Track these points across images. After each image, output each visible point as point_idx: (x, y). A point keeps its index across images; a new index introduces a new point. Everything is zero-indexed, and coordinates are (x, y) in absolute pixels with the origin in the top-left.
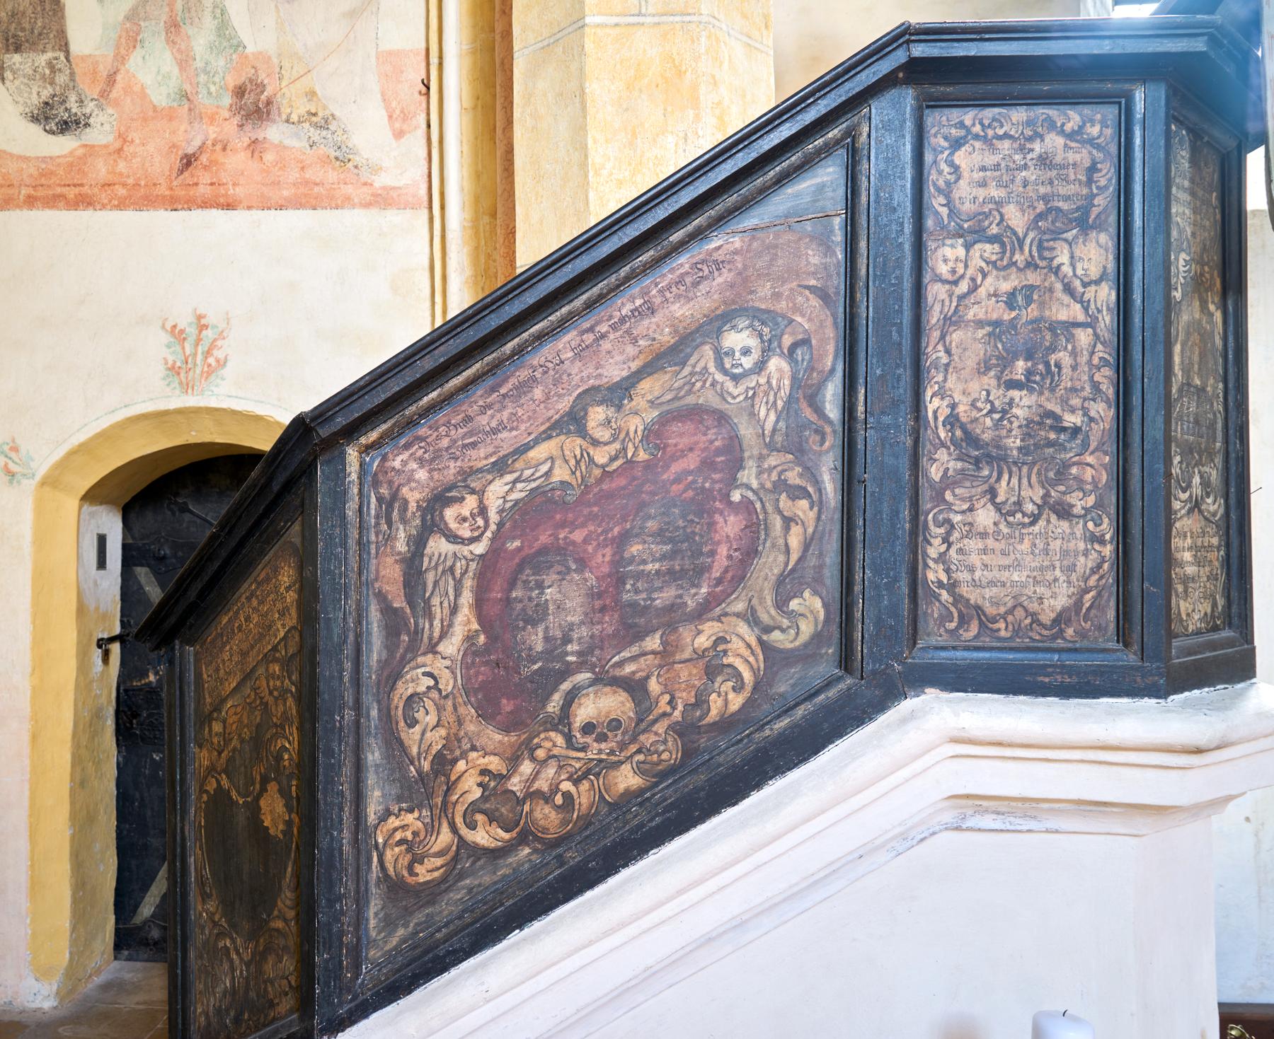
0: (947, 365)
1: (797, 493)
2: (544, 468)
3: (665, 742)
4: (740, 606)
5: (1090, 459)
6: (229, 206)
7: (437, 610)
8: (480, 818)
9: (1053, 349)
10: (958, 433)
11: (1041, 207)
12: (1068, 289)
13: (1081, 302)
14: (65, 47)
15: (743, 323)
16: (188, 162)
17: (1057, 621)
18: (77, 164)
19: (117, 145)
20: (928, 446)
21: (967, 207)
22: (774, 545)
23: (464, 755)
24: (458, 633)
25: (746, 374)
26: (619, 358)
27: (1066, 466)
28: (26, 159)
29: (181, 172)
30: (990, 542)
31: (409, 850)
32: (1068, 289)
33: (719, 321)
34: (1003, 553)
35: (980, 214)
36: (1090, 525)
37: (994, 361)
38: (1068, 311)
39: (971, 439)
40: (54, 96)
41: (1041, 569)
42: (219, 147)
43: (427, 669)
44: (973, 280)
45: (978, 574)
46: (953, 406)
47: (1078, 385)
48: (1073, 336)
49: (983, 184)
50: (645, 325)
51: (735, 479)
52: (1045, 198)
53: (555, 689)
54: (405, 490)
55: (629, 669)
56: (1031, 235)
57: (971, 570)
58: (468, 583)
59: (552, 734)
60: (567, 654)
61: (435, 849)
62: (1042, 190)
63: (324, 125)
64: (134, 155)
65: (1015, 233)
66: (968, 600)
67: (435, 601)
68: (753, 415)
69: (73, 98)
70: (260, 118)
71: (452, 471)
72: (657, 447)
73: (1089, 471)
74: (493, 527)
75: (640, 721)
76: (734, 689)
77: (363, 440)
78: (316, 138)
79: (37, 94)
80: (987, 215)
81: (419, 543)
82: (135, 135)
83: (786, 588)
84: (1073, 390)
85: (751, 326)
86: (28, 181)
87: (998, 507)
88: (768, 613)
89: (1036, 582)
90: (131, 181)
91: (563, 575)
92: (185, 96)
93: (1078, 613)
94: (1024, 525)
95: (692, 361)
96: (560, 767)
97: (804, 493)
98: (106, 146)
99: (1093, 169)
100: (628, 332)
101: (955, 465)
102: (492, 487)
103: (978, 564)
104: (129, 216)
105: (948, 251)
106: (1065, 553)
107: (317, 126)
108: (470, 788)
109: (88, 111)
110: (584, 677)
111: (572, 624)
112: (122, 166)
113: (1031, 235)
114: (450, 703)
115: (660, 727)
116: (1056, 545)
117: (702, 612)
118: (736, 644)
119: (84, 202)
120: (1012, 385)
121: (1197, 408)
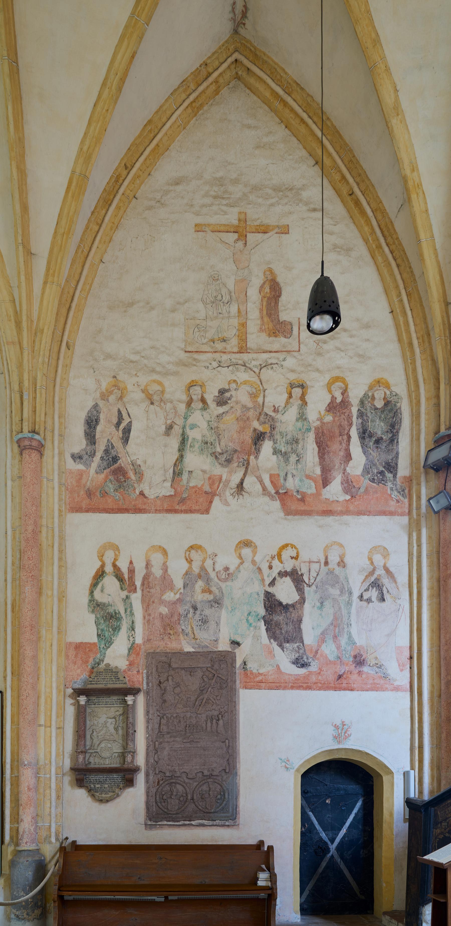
6: (352, 690)
14: (302, 642)
16: (340, 677)
18: (306, 677)
19: (319, 671)
28: (291, 675)
29: (338, 680)
42: (349, 673)
63: (380, 667)
64: (324, 674)
69: (305, 657)
70: (361, 665)
78: (378, 671)
82: (324, 669)
86: (291, 682)
90: (323, 682)
92: (339, 658)
98: (315, 672)
104: (322, 692)
107: (378, 667)
109: (310, 661)
112: (320, 678)
119: (309, 688)
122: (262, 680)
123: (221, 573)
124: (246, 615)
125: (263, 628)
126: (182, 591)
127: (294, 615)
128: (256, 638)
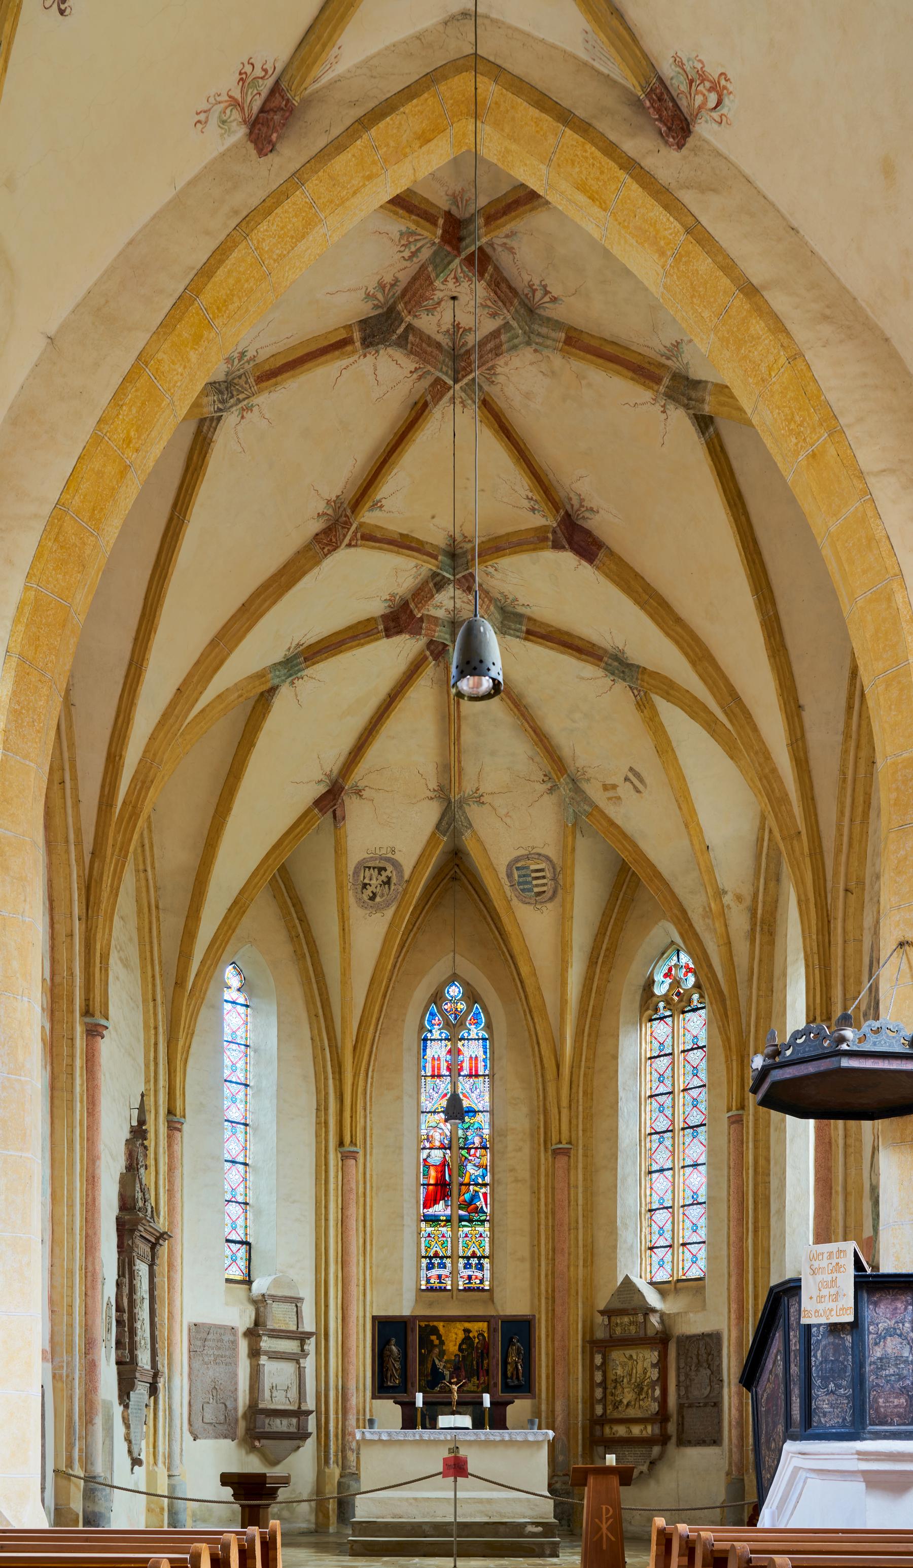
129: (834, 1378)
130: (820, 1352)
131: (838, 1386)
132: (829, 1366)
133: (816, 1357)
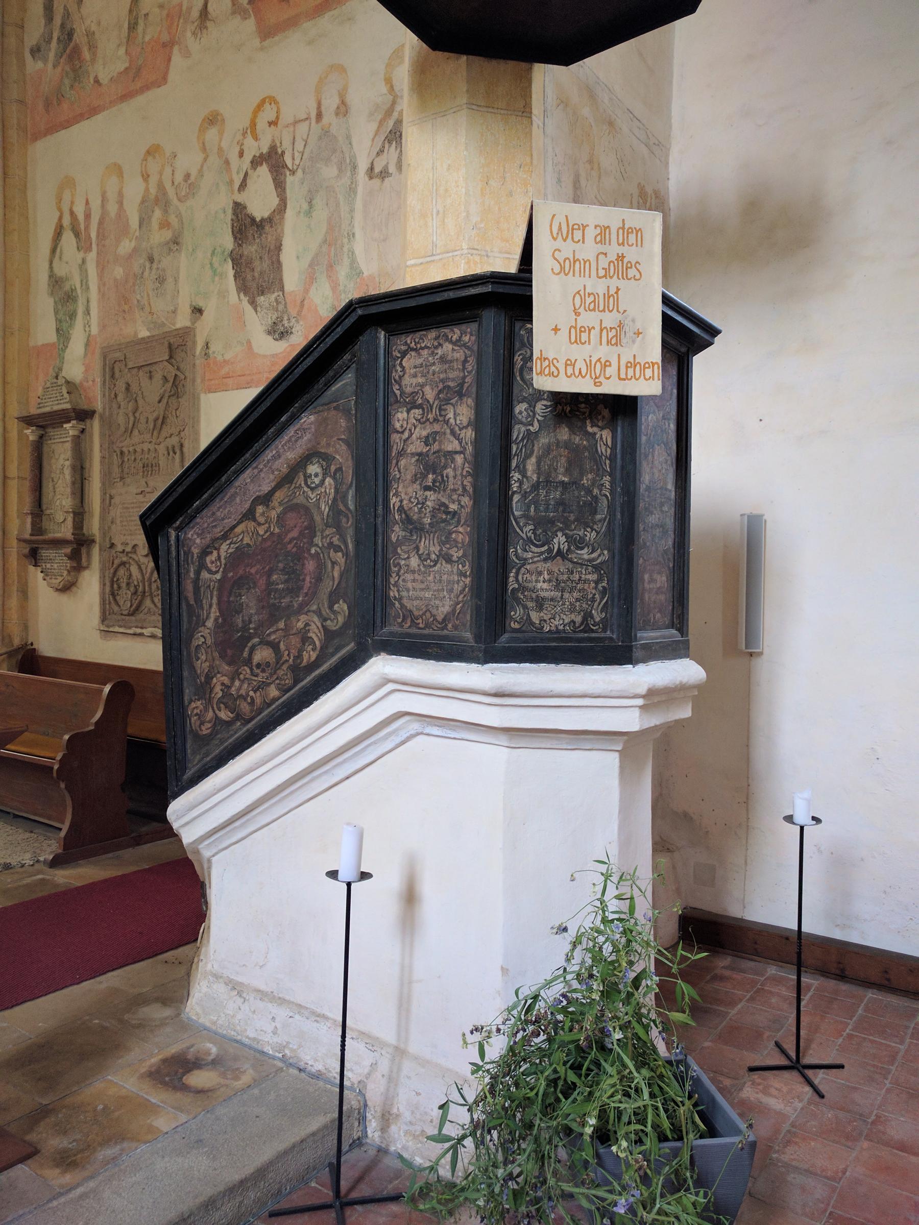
0: (399, 478)
1: (337, 549)
2: (241, 537)
3: (287, 675)
4: (314, 607)
5: (461, 529)
7: (205, 606)
8: (222, 706)
9: (445, 467)
10: (403, 516)
11: (441, 386)
12: (453, 433)
13: (458, 439)
15: (315, 460)
17: (444, 620)
20: (391, 523)
21: (408, 390)
22: (328, 576)
23: (215, 675)
24: (212, 616)
25: (317, 486)
26: (267, 481)
27: (450, 533)
30: (416, 575)
31: (199, 718)
32: (453, 433)
33: (306, 460)
34: (422, 582)
35: (413, 393)
36: (460, 566)
37: (419, 476)
38: (453, 445)
39: (408, 520)
40: (278, 318)
41: (438, 590)
43: (202, 634)
44: (410, 430)
45: (411, 593)
46: (401, 501)
47: (456, 486)
48: (454, 459)
49: (415, 376)
50: (277, 464)
51: (312, 542)
52: (442, 381)
53: (246, 646)
54: (193, 548)
55: (273, 637)
56: (436, 403)
57: (408, 590)
58: (215, 593)
59: (246, 667)
60: (250, 629)
61: (208, 719)
62: (442, 376)
65: (428, 402)
66: (406, 607)
67: (204, 602)
68: (319, 508)
69: (286, 318)
71: (209, 539)
72: (282, 526)
73: (461, 536)
74: (223, 566)
75: (278, 663)
76: (312, 649)
77: (174, 525)
79: (271, 317)
80: (417, 393)
81: (198, 573)
83: (333, 598)
84: (454, 490)
85: (318, 461)
87: (420, 557)
88: (326, 611)
89: (436, 598)
91: (249, 589)
93: (454, 615)
94: (431, 567)
95: (295, 481)
96: (249, 684)
97: (340, 550)
99: (465, 361)
100: (271, 468)
101: (402, 534)
102: (222, 547)
103: (411, 588)
105: (399, 415)
106: (449, 582)
108: (218, 692)
109: (291, 324)
110: (256, 640)
111: (251, 614)
113: (436, 403)
114: (210, 650)
115: (285, 667)
116: (445, 577)
117: (300, 610)
118: (313, 627)
120: (427, 488)
121: (562, 494)
122: (228, 373)
123: (182, 186)
124: (209, 254)
125: (231, 273)
126: (137, 234)
127: (269, 238)
128: (223, 294)
129: (567, 525)
130: (533, 460)
131: (580, 543)
132: (556, 494)
133: (523, 473)
